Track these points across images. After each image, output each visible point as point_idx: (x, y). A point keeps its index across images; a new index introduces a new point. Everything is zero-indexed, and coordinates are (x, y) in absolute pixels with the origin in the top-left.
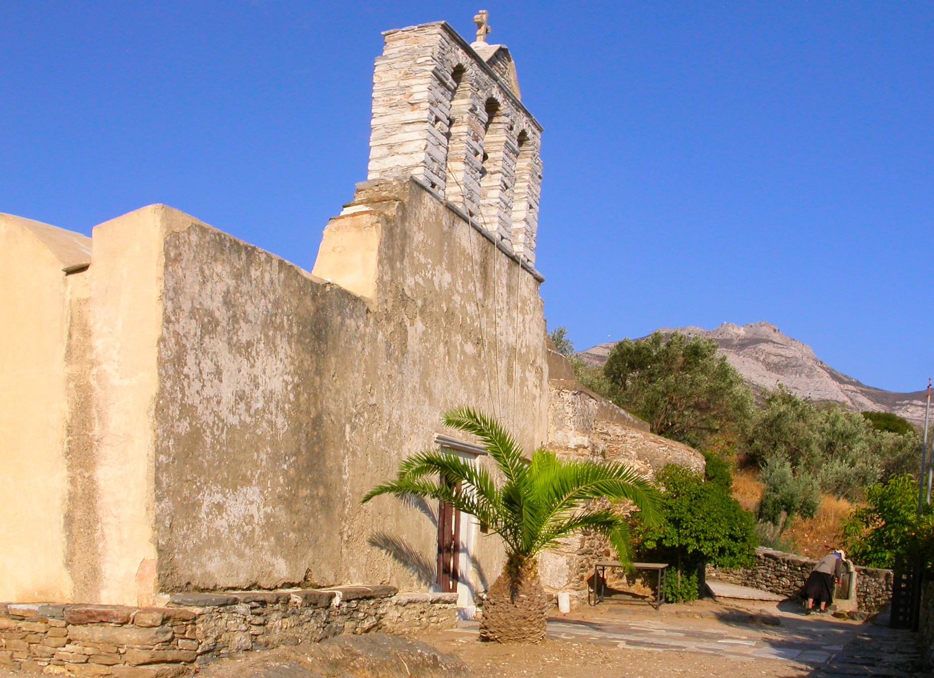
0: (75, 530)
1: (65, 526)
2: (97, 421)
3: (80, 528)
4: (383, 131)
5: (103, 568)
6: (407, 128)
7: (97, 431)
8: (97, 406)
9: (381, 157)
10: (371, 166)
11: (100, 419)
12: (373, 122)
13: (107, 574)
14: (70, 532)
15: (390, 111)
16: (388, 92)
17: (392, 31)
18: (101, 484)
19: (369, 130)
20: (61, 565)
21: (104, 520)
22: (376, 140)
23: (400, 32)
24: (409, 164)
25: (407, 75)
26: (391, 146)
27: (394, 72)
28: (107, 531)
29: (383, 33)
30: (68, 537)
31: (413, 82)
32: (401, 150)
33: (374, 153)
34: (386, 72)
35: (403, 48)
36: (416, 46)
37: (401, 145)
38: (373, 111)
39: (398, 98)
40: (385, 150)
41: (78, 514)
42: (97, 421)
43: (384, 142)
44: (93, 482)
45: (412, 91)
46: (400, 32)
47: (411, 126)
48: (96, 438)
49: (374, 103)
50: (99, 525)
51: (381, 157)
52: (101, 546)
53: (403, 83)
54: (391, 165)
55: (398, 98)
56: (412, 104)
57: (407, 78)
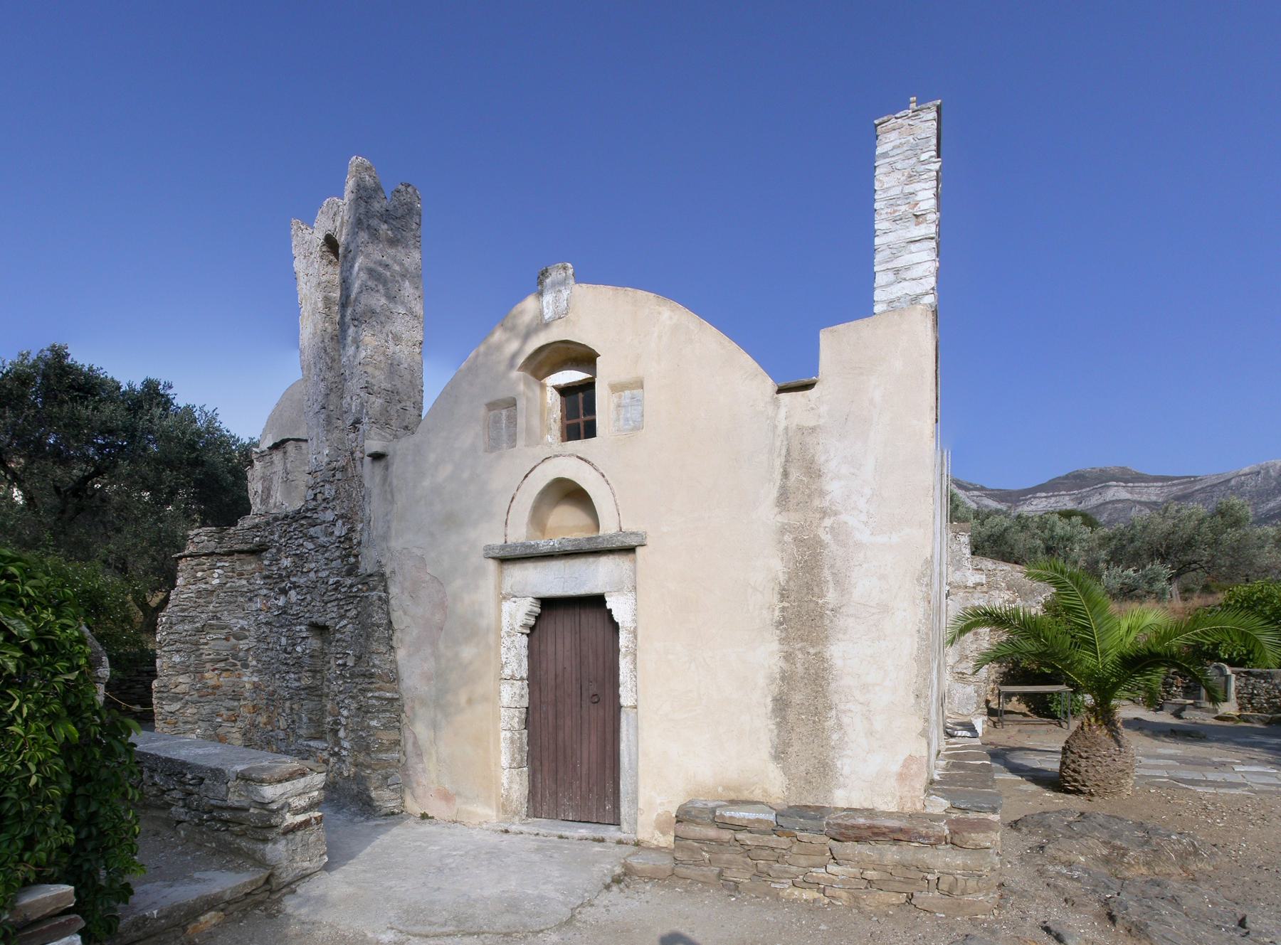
0: (792, 717)
1: (773, 711)
2: (831, 585)
3: (800, 714)
4: (888, 252)
5: (839, 764)
6: (913, 247)
7: (831, 597)
8: (832, 566)
9: (889, 285)
10: (878, 295)
11: (837, 583)
12: (877, 241)
13: (846, 771)
14: (784, 718)
15: (894, 226)
16: (892, 201)
17: (885, 118)
18: (838, 662)
19: (871, 250)
20: (766, 756)
21: (841, 707)
22: (880, 264)
23: (894, 120)
24: (919, 292)
25: (911, 178)
26: (897, 271)
27: (897, 175)
28: (846, 720)
29: (876, 122)
30: (778, 724)
31: (917, 186)
32: (908, 275)
33: (880, 279)
34: (886, 174)
35: (898, 142)
36: (910, 138)
37: (907, 269)
38: (876, 227)
39: (903, 208)
40: (890, 277)
41: (797, 698)
42: (831, 585)
43: (890, 266)
44: (823, 660)
45: (918, 198)
46: (894, 120)
47: (918, 244)
48: (830, 607)
49: (877, 217)
50: (834, 712)
51: (889, 285)
52: (835, 737)
53: (908, 189)
54: (899, 294)
55: (903, 208)
56: (916, 216)
57: (911, 183)
